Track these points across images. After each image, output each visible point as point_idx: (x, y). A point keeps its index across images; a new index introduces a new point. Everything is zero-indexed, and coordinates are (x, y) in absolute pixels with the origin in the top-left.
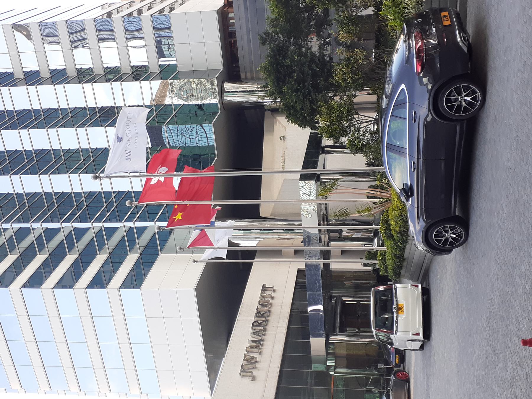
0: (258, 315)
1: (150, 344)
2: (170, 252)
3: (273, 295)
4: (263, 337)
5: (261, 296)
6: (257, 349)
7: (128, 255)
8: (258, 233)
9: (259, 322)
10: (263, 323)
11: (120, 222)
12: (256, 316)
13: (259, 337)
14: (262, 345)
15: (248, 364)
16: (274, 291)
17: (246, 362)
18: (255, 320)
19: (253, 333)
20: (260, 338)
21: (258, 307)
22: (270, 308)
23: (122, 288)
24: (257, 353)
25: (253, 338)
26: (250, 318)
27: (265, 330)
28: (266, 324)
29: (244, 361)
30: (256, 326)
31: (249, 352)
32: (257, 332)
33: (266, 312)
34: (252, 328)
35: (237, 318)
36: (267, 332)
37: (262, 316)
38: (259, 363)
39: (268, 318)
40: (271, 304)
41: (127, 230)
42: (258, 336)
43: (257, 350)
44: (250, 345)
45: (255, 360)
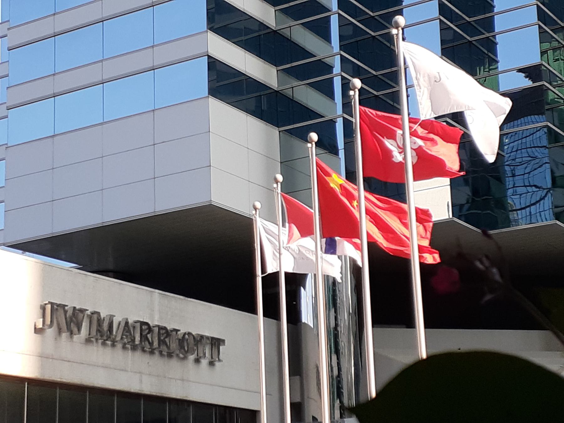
0: (162, 332)
1: (102, 121)
2: (285, 150)
3: (204, 362)
4: (119, 346)
5: (202, 337)
6: (97, 334)
7: (275, 66)
8: (329, 323)
9: (149, 336)
10: (147, 343)
11: (342, 47)
12: (160, 328)
13: (120, 337)
14: (104, 344)
15: (66, 319)
16: (211, 364)
17: (70, 313)
18: (154, 327)
19: (127, 321)
20: (118, 338)
21: (179, 333)
22: (177, 355)
23: (208, 58)
24: (89, 334)
25: (117, 324)
26: (157, 317)
27: (134, 348)
28: (145, 348)
29: (72, 309)
30: (141, 327)
31: (90, 317)
32: (130, 331)
33: (168, 347)
34: (136, 322)
35: (157, 291)
36: (130, 351)
37: (161, 342)
38: (70, 340)
39: (157, 352)
40: (185, 358)
41: (328, 61)
42: (123, 335)
43: (95, 334)
44: (104, 320)
45: (75, 330)
